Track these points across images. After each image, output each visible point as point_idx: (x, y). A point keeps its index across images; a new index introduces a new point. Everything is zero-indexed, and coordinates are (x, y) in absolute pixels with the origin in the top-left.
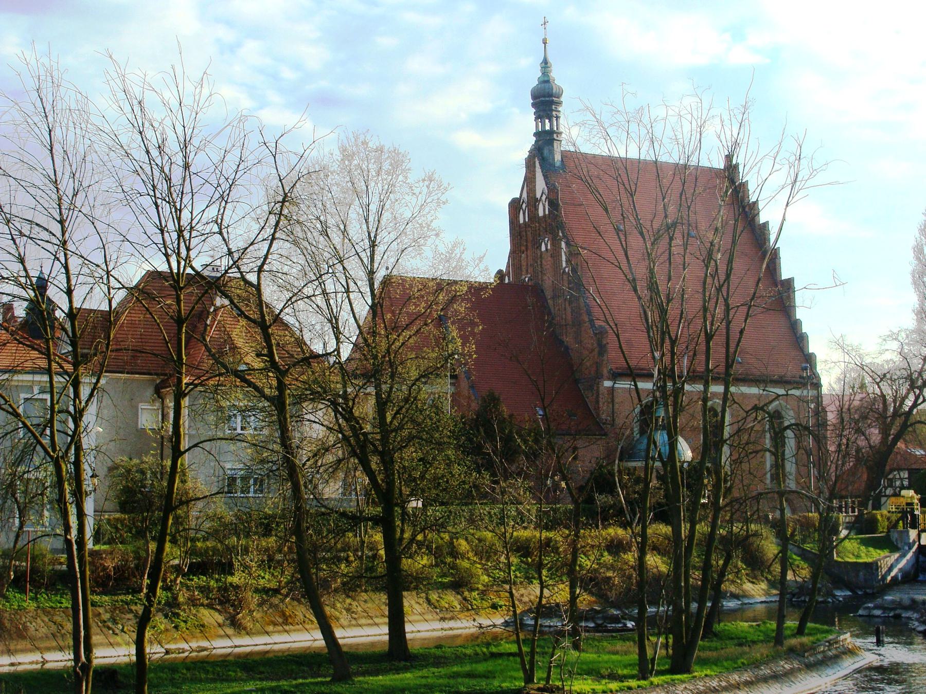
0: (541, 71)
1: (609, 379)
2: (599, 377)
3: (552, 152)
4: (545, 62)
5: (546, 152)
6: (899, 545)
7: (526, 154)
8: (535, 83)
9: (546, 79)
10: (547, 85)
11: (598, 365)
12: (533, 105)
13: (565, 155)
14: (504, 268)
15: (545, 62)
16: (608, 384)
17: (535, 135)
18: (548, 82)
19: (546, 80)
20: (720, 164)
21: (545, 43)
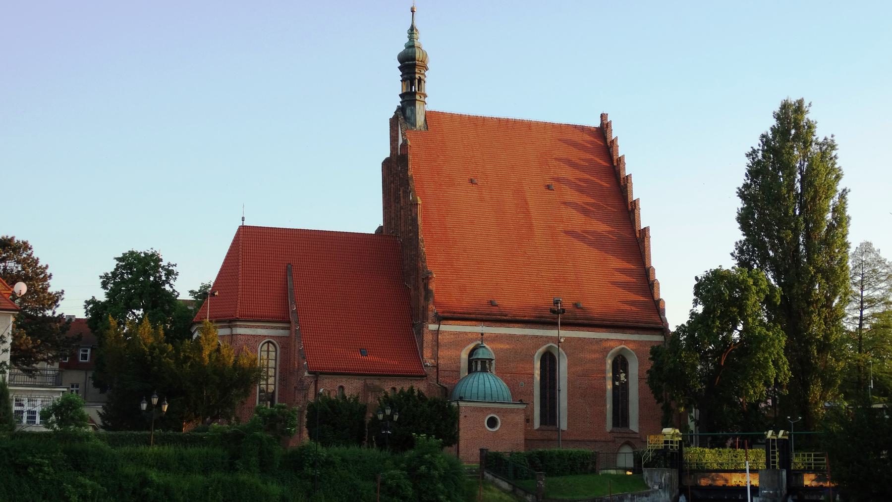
0: (409, 37)
1: (434, 323)
2: (425, 319)
3: (414, 112)
4: (412, 29)
5: (408, 112)
6: (649, 485)
7: (392, 115)
8: (402, 48)
9: (411, 44)
10: (410, 50)
11: (425, 309)
12: (400, 68)
13: (429, 116)
14: (382, 225)
15: (412, 29)
16: (433, 327)
17: (401, 96)
18: (413, 46)
19: (411, 46)
20: (596, 123)
21: (413, 11)
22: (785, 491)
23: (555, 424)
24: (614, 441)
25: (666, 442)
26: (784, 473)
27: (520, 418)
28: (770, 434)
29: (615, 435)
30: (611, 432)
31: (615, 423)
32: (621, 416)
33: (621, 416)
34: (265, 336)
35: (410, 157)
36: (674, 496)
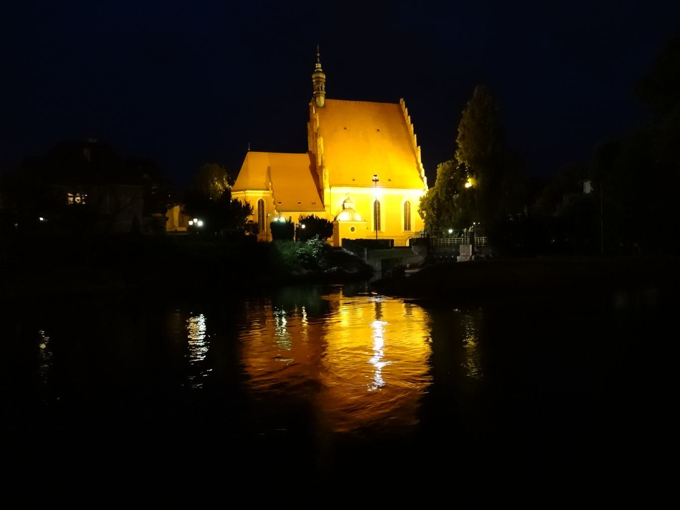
3: (319, 100)
5: (317, 100)
6: (415, 252)
22: (471, 254)
23: (379, 229)
24: (404, 236)
25: (422, 235)
26: (471, 246)
27: (364, 228)
28: (465, 230)
29: (405, 233)
30: (404, 232)
31: (405, 229)
32: (407, 227)
33: (407, 227)
34: (259, 197)
35: (318, 119)
36: (425, 256)
